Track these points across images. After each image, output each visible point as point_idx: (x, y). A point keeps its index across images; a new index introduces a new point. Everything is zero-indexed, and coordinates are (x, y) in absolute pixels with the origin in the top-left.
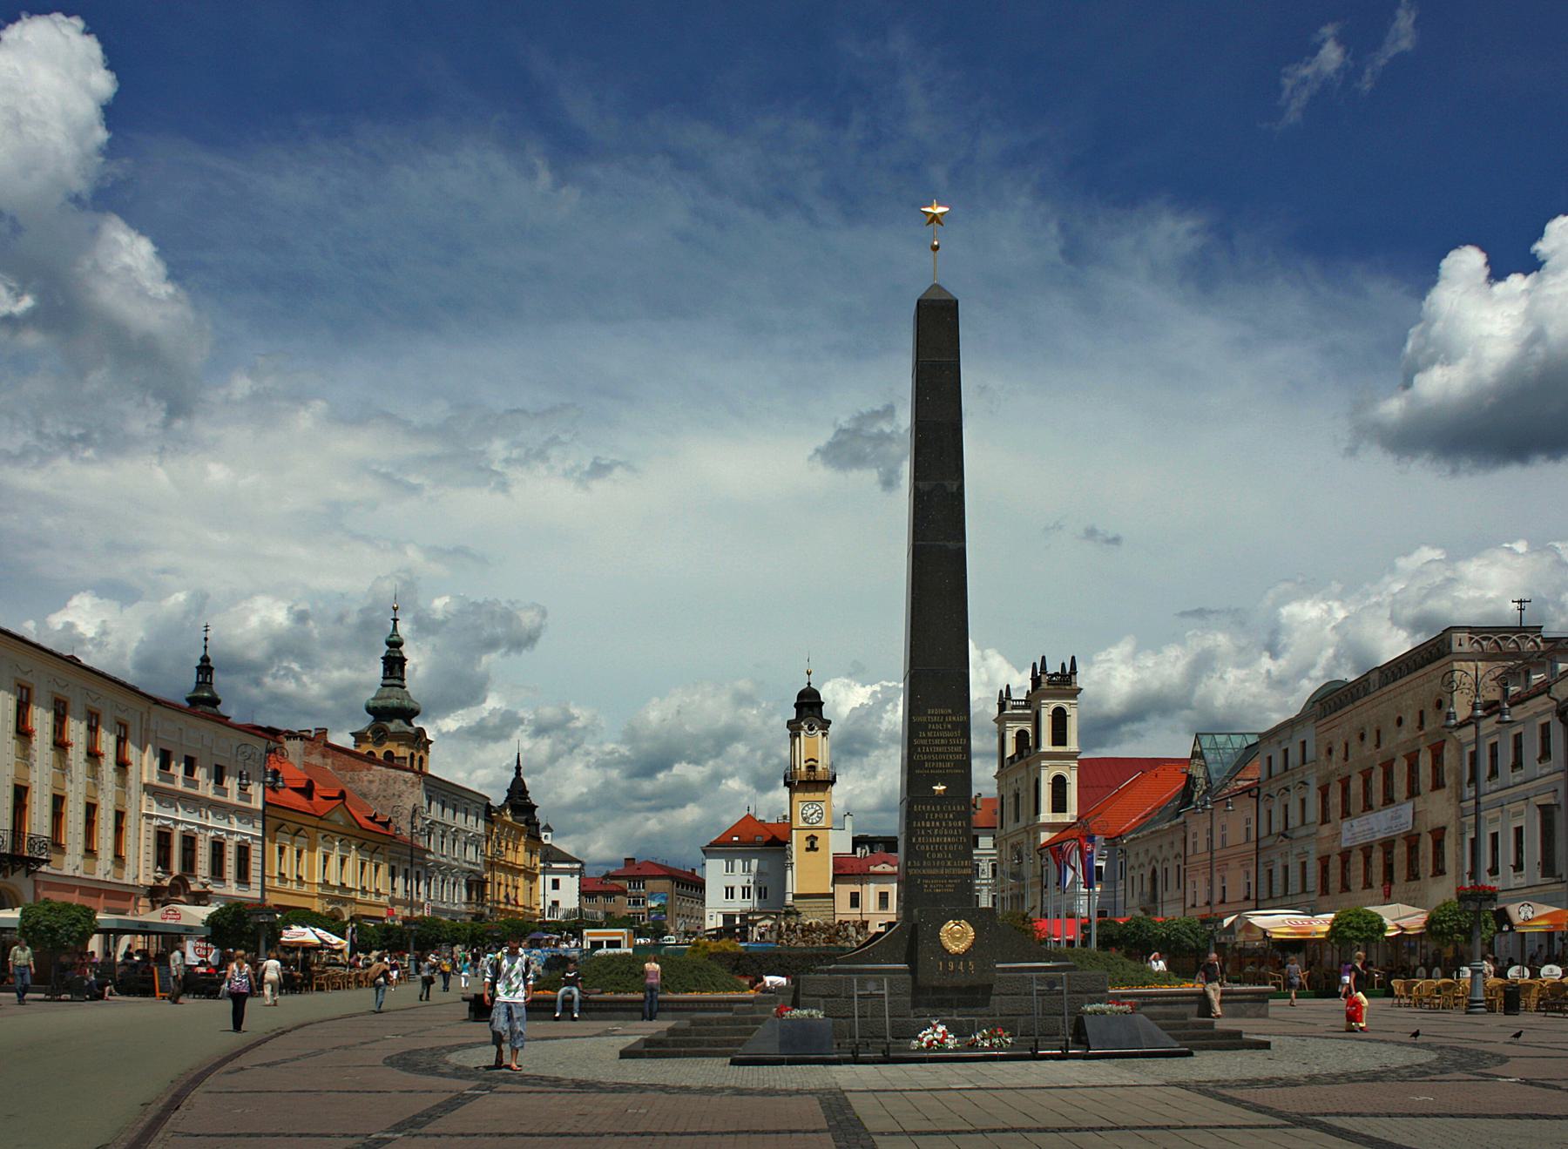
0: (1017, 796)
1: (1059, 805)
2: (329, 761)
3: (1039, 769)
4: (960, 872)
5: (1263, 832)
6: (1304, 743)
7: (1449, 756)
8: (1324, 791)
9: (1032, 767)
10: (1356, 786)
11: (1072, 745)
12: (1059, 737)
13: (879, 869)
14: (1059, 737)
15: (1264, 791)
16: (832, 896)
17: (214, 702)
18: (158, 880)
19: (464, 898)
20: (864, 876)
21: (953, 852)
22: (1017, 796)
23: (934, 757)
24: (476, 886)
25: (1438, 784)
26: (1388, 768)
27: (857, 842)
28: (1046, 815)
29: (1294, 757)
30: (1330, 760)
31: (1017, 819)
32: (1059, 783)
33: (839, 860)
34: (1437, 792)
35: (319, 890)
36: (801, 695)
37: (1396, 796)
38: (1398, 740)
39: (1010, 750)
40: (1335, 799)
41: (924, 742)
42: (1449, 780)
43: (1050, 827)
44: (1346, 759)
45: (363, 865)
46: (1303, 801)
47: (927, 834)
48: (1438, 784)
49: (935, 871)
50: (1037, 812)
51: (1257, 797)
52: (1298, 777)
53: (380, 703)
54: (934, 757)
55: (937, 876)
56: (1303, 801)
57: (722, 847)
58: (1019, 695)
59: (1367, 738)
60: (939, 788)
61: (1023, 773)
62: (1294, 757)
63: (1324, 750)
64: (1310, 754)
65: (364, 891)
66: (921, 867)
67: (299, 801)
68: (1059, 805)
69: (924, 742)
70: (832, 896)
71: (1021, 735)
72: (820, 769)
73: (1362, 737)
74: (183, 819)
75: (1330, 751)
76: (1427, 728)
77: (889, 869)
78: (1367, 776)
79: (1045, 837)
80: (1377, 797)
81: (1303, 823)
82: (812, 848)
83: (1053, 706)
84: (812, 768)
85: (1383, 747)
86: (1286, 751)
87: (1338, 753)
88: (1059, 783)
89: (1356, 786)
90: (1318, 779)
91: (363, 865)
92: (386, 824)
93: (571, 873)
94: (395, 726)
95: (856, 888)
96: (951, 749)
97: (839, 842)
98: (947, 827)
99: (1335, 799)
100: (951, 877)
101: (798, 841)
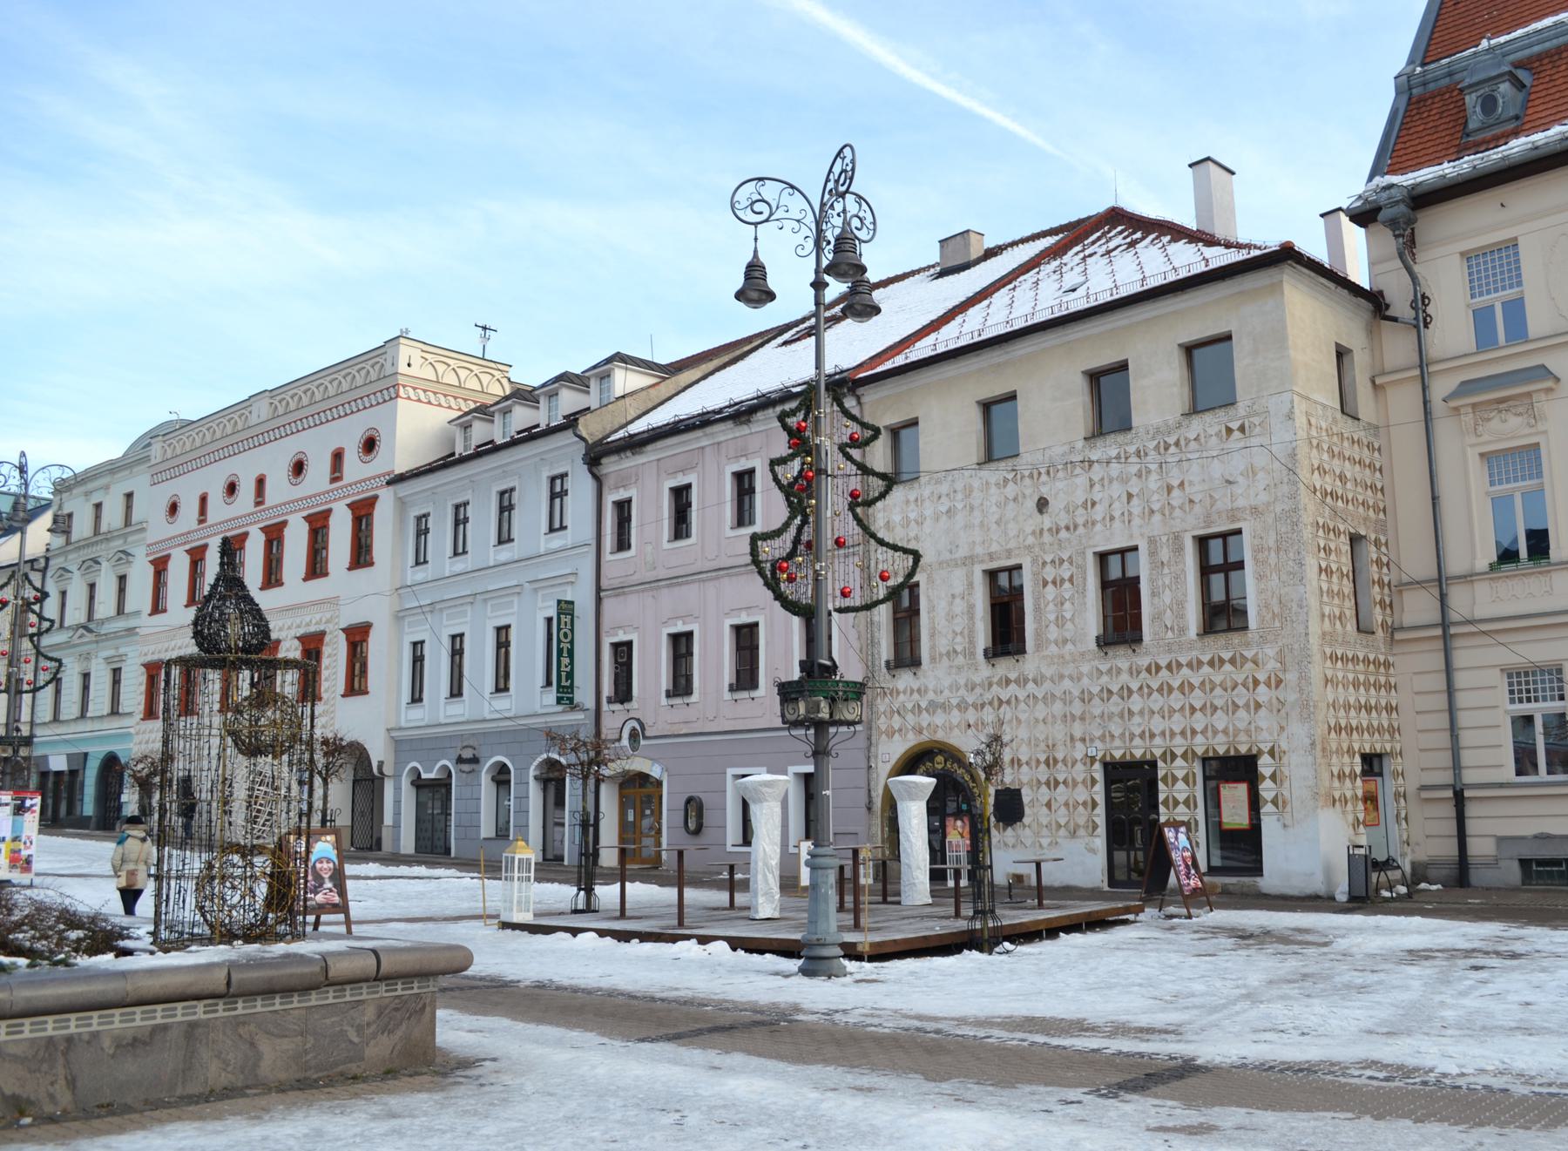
8: (160, 566)
15: (55, 563)
46: (122, 579)
62: (113, 516)
86: (98, 506)
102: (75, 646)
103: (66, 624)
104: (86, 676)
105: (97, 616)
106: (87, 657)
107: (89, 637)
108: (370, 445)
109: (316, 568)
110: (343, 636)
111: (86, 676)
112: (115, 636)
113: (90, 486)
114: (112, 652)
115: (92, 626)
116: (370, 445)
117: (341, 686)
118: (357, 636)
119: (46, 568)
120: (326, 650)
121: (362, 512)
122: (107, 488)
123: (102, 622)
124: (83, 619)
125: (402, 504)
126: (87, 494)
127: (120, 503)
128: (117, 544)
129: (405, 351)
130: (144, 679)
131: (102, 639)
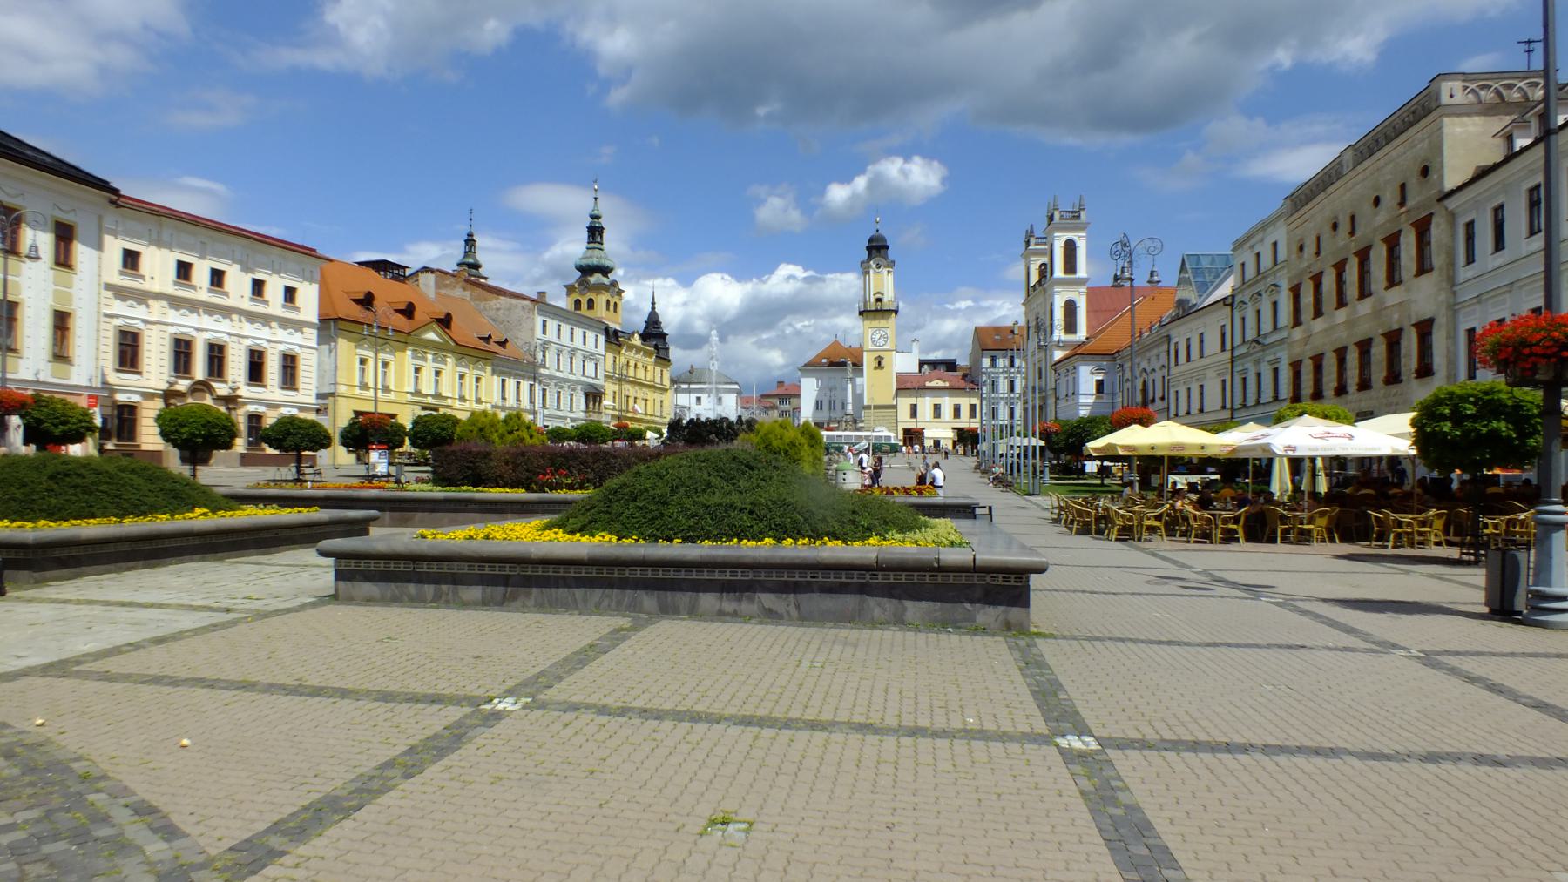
2: (467, 293)
3: (1052, 296)
5: (1238, 340)
6: (1275, 244)
7: (1437, 232)
8: (1296, 291)
10: (1329, 282)
11: (1082, 271)
12: (1070, 266)
13: (935, 383)
14: (1070, 266)
15: (1238, 299)
16: (895, 407)
17: (476, 266)
18: (171, 384)
19: (583, 407)
20: (921, 390)
24: (594, 396)
25: (1423, 268)
26: (1364, 255)
27: (922, 363)
28: (1059, 334)
29: (1266, 261)
30: (1300, 258)
32: (1070, 307)
33: (901, 378)
34: (1424, 278)
35: (409, 397)
36: (871, 240)
37: (1373, 287)
38: (1376, 223)
39: (1034, 279)
40: (1307, 299)
42: (1438, 259)
44: (1318, 254)
45: (462, 377)
46: (1275, 304)
48: (1423, 268)
51: (1232, 305)
52: (1270, 280)
53: (584, 262)
56: (1275, 304)
57: (811, 367)
59: (1340, 228)
62: (1266, 261)
63: (1295, 248)
64: (1282, 255)
65: (462, 399)
67: (401, 321)
68: (1071, 327)
70: (895, 407)
72: (885, 300)
73: (1335, 226)
74: (203, 329)
75: (1301, 248)
76: (1410, 203)
77: (940, 384)
78: (1340, 267)
79: (1058, 355)
80: (1352, 290)
81: (1275, 328)
82: (880, 366)
83: (1064, 239)
84: (879, 300)
85: (1358, 233)
86: (1258, 255)
87: (1310, 249)
88: (1070, 307)
89: (1329, 282)
90: (1290, 280)
91: (462, 377)
92: (503, 344)
93: (730, 391)
94: (595, 278)
95: (913, 401)
97: (906, 363)
99: (1307, 299)
101: (868, 361)
104: (1259, 375)
106: (1257, 362)
107: (1259, 347)
108: (1425, 172)
109: (1393, 281)
111: (1259, 375)
112: (1272, 345)
113: (1253, 241)
116: (1425, 172)
118: (1425, 329)
120: (1404, 343)
121: (1422, 228)
122: (1262, 240)
123: (1266, 336)
126: (1252, 247)
129: (1446, 87)
131: (1265, 347)
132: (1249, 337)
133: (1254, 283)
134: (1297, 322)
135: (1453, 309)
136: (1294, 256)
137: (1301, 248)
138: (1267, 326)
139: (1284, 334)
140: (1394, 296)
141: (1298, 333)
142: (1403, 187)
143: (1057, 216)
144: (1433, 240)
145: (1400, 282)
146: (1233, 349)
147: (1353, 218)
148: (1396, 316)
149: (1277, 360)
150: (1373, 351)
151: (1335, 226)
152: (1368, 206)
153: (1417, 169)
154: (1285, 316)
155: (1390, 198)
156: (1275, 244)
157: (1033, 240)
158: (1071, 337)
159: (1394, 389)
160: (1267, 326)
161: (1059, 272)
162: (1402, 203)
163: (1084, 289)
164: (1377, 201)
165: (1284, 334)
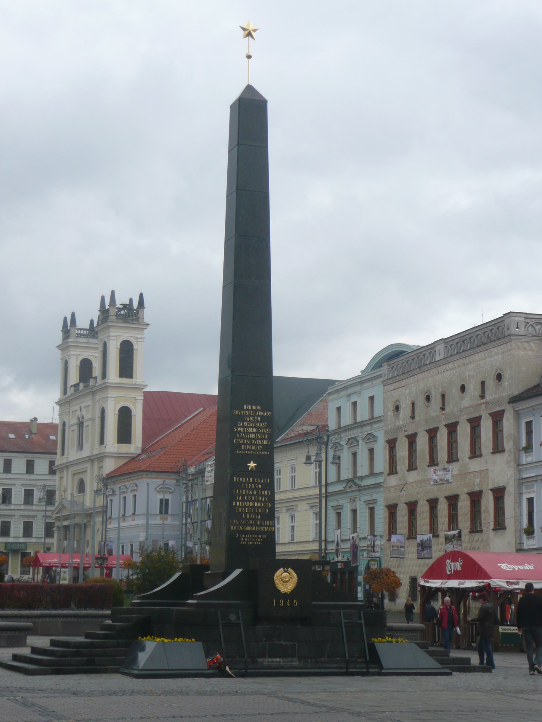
0: (81, 425)
1: (124, 435)
4: (266, 529)
6: (372, 398)
8: (392, 444)
9: (98, 397)
10: (422, 442)
14: (126, 368)
21: (261, 514)
22: (81, 425)
23: (249, 442)
26: (452, 428)
30: (397, 417)
31: (80, 446)
32: (125, 415)
37: (460, 455)
38: (463, 406)
39: (74, 377)
40: (402, 451)
41: (241, 430)
42: (508, 445)
43: (117, 456)
46: (371, 451)
47: (243, 500)
48: (498, 449)
49: (249, 528)
50: (102, 442)
54: (249, 442)
55: (251, 532)
56: (371, 451)
58: (83, 323)
59: (433, 400)
60: (252, 465)
61: (88, 401)
63: (391, 407)
64: (378, 411)
66: (239, 525)
69: (241, 430)
71: (86, 367)
75: (397, 408)
78: (432, 433)
80: (442, 454)
85: (448, 410)
86: (355, 404)
87: (406, 411)
88: (125, 415)
89: (422, 442)
90: (386, 433)
96: (260, 436)
98: (258, 495)
99: (402, 451)
100: (261, 533)
102: (347, 492)
103: (342, 479)
104: (354, 512)
105: (359, 474)
107: (354, 488)
108: (499, 377)
109: (475, 453)
110: (491, 493)
111: (354, 512)
112: (368, 487)
114: (368, 498)
115: (357, 481)
117: (492, 526)
118: (499, 494)
119: (328, 441)
120: (483, 502)
123: (362, 478)
124: (350, 476)
125: (518, 415)
126: (349, 396)
127: (367, 402)
128: (367, 430)
130: (387, 514)
131: (361, 489)
132: (343, 477)
133: (348, 428)
134: (393, 470)
135: (522, 482)
136: (390, 413)
137: (397, 408)
138: (363, 470)
139: (380, 480)
140: (475, 465)
141: (393, 481)
142: (483, 383)
143: (113, 312)
144: (505, 430)
145: (481, 456)
146: (327, 485)
147: (443, 396)
148: (477, 481)
149: (374, 501)
150: (460, 504)
151: (428, 398)
152: (455, 390)
153: (493, 374)
154: (381, 462)
155: (473, 389)
156: (372, 398)
157: (74, 332)
158: (125, 448)
159: (476, 536)
160: (363, 470)
161: (113, 376)
162: (482, 397)
163: (140, 397)
164: (463, 388)
165: (380, 480)
